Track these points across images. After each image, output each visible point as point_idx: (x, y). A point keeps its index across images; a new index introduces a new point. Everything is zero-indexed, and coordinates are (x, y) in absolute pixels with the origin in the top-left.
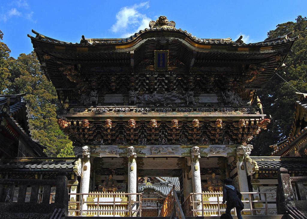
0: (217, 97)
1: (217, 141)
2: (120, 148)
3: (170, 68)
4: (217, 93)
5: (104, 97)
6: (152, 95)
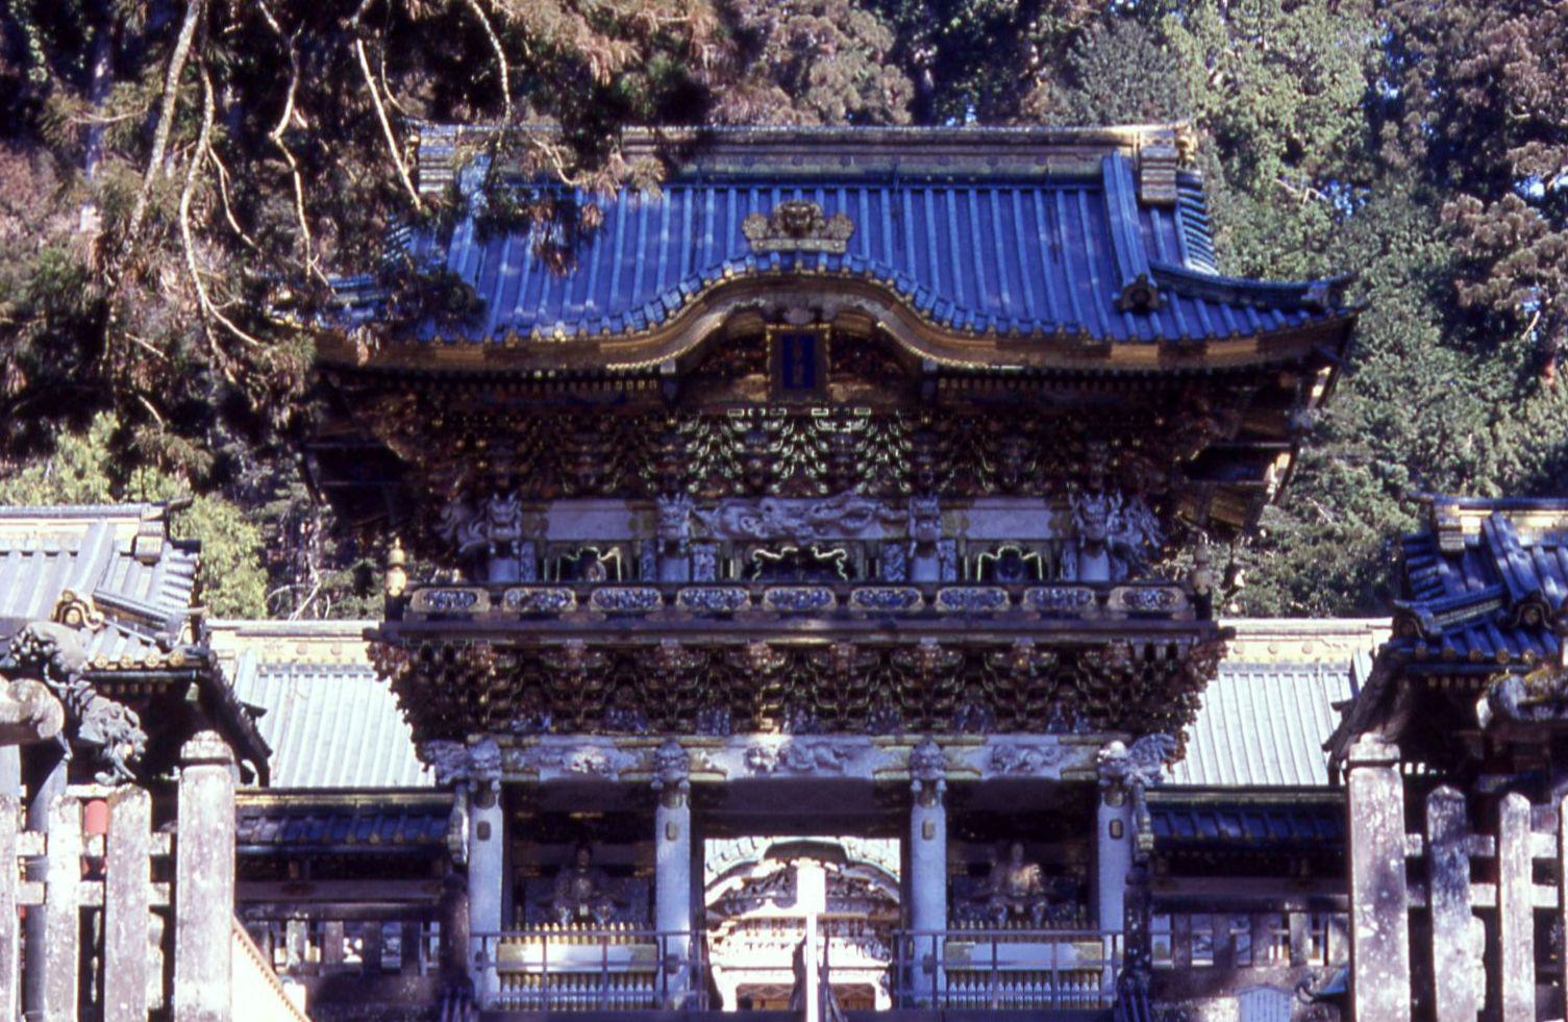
1: (1019, 718)
2: (621, 748)
3: (838, 391)
4: (1048, 496)
5: (545, 511)
6: (756, 505)
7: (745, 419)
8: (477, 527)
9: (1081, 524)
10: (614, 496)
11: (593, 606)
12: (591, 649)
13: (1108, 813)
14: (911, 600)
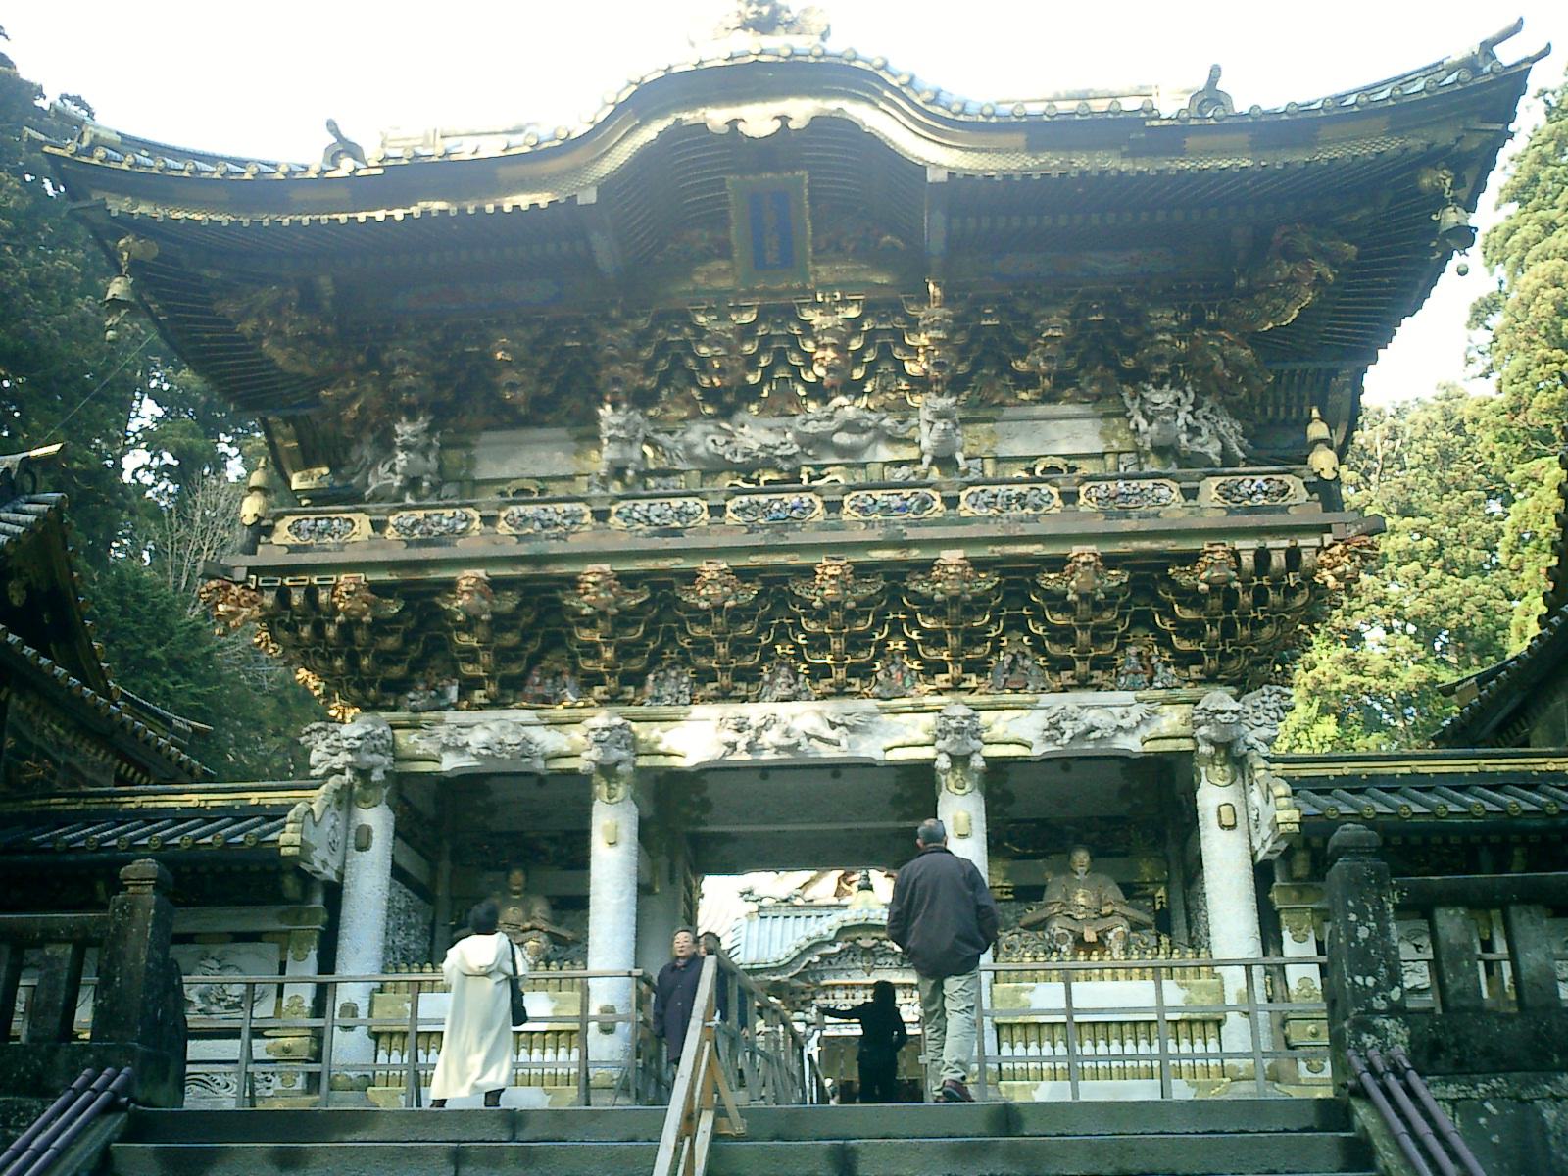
0: (1101, 423)
1: (1081, 667)
3: (824, 272)
4: (1097, 399)
7: (708, 311)
8: (387, 466)
9: (1143, 425)
10: (559, 424)
11: (503, 528)
12: (497, 585)
13: (1212, 795)
14: (925, 503)
